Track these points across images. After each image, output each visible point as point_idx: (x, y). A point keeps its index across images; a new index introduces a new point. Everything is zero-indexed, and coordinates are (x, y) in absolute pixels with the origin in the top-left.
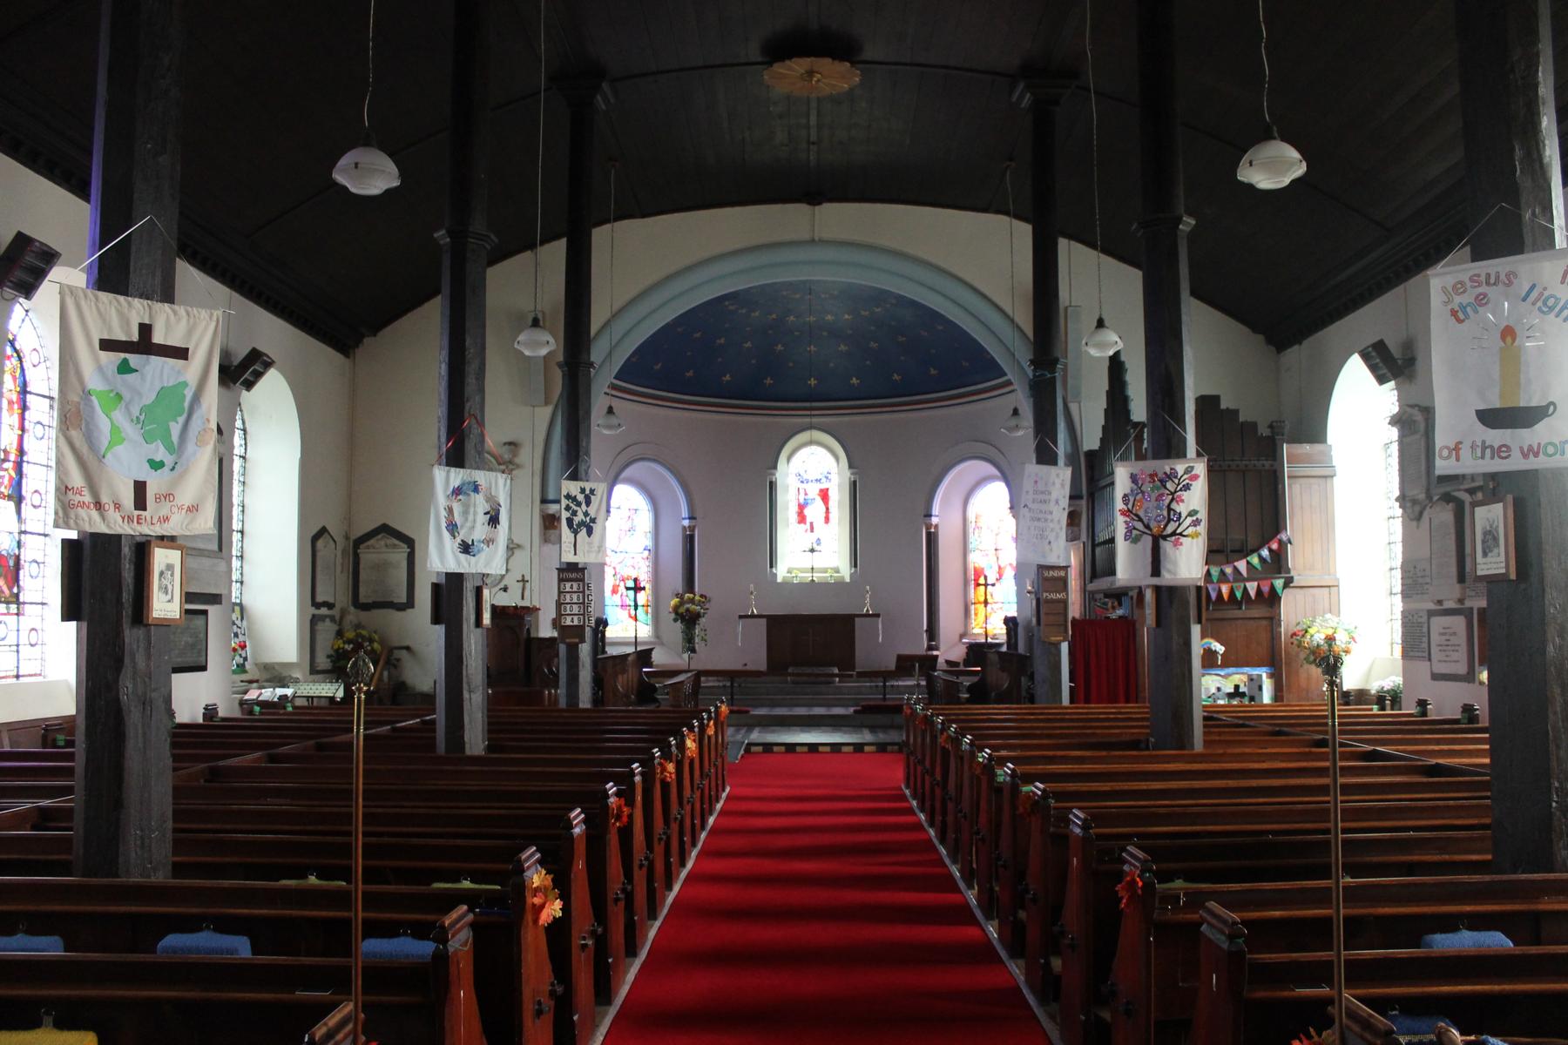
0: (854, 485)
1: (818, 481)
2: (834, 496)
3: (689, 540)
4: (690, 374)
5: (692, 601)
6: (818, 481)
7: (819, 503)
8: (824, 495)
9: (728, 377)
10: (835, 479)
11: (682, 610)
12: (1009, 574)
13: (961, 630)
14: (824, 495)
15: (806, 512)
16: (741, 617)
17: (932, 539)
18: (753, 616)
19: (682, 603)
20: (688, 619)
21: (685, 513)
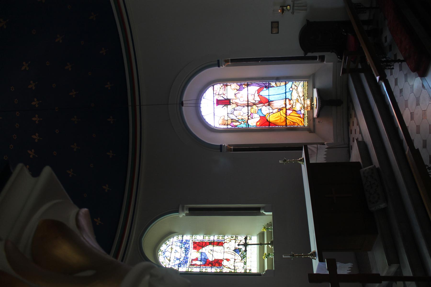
0: (193, 212)
1: (187, 250)
2: (199, 238)
6: (187, 250)
7: (206, 250)
8: (199, 245)
10: (187, 237)
12: (265, 93)
13: (307, 133)
14: (199, 245)
15: (211, 259)
17: (238, 148)
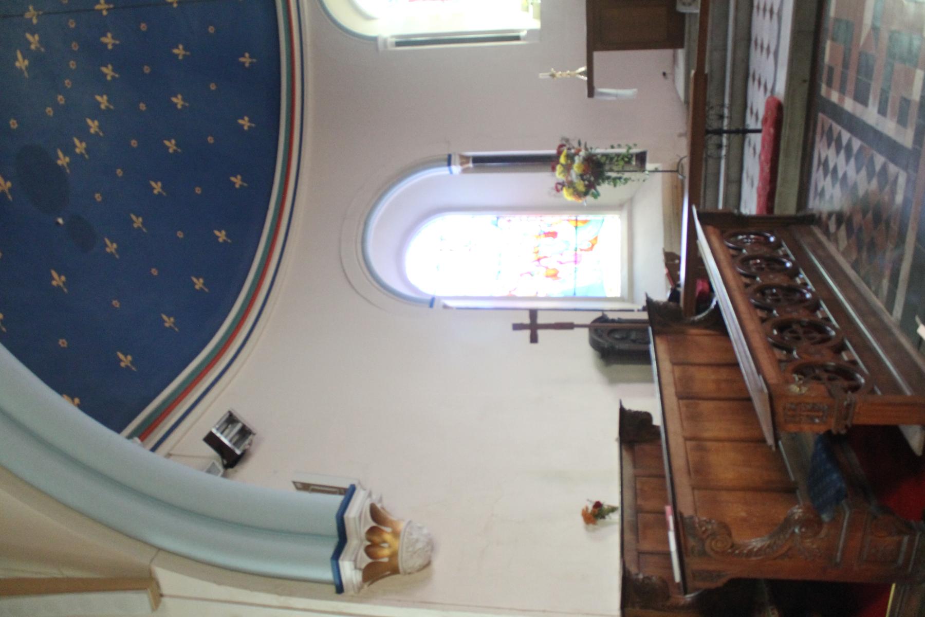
3: (481, 162)
4: (237, 181)
5: (568, 168)
9: (245, 123)
11: (581, 186)
16: (591, 92)
18: (590, 73)
19: (571, 185)
20: (596, 170)
21: (443, 171)
